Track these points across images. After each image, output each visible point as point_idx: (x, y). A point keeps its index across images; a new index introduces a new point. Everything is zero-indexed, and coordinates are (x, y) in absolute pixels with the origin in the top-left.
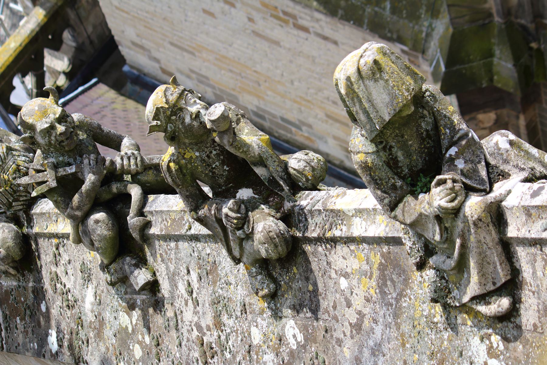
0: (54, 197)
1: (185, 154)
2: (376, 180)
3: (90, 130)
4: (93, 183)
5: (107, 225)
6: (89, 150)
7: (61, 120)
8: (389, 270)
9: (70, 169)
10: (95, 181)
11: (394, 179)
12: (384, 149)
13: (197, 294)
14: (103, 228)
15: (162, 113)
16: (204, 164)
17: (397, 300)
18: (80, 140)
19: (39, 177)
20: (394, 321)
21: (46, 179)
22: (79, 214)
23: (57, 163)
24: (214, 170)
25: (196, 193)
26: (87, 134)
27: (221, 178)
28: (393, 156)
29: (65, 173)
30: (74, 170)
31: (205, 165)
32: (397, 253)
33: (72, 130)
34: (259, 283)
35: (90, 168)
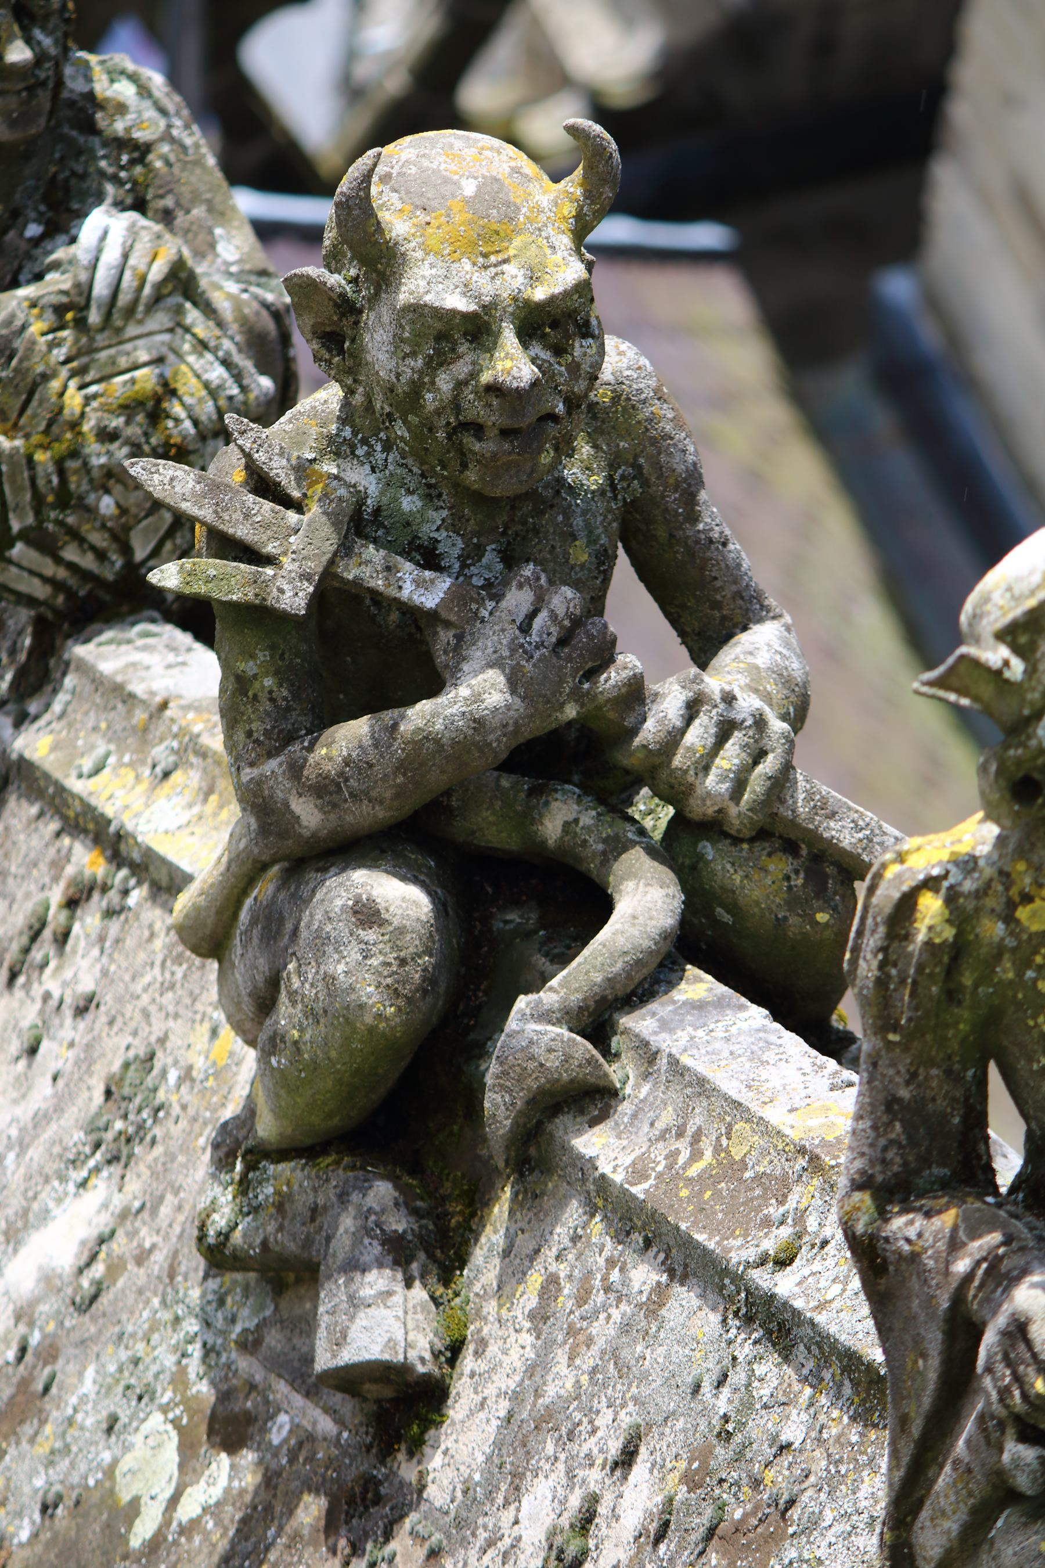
0: (253, 656)
1: (1027, 899)
4: (479, 724)
5: (403, 962)
6: (566, 556)
7: (541, 326)
10: (496, 722)
14: (375, 962)
18: (561, 481)
19: (247, 516)
21: (270, 548)
23: (377, 511)
26: (610, 478)
29: (379, 583)
30: (430, 601)
33: (560, 408)
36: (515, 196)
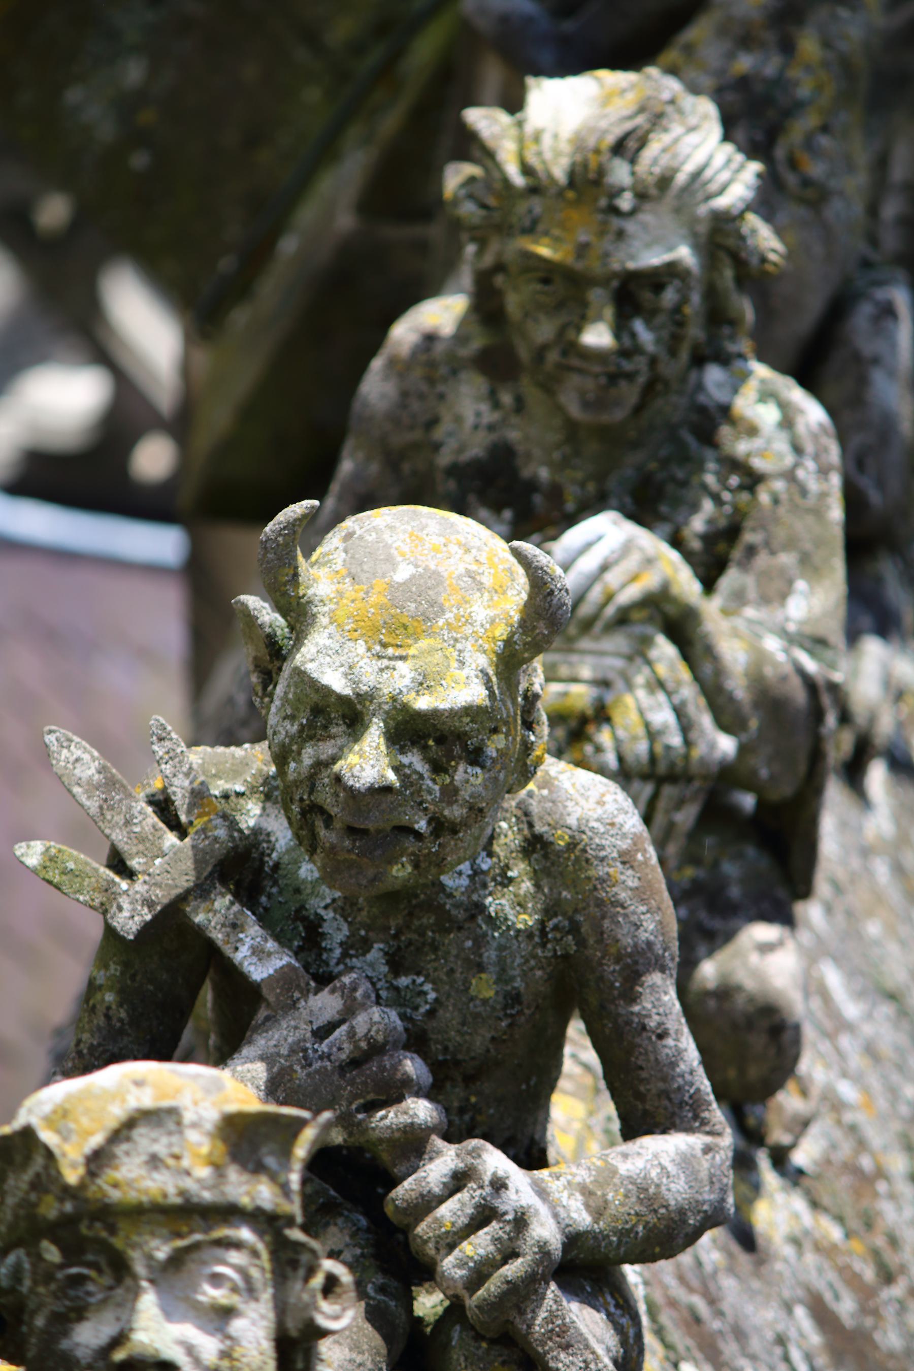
3: (574, 929)
7: (427, 736)
18: (480, 908)
19: (127, 823)
21: (135, 863)
23: (277, 866)
26: (542, 923)
29: (218, 936)
30: (258, 972)
35: (297, 1048)
36: (449, 600)
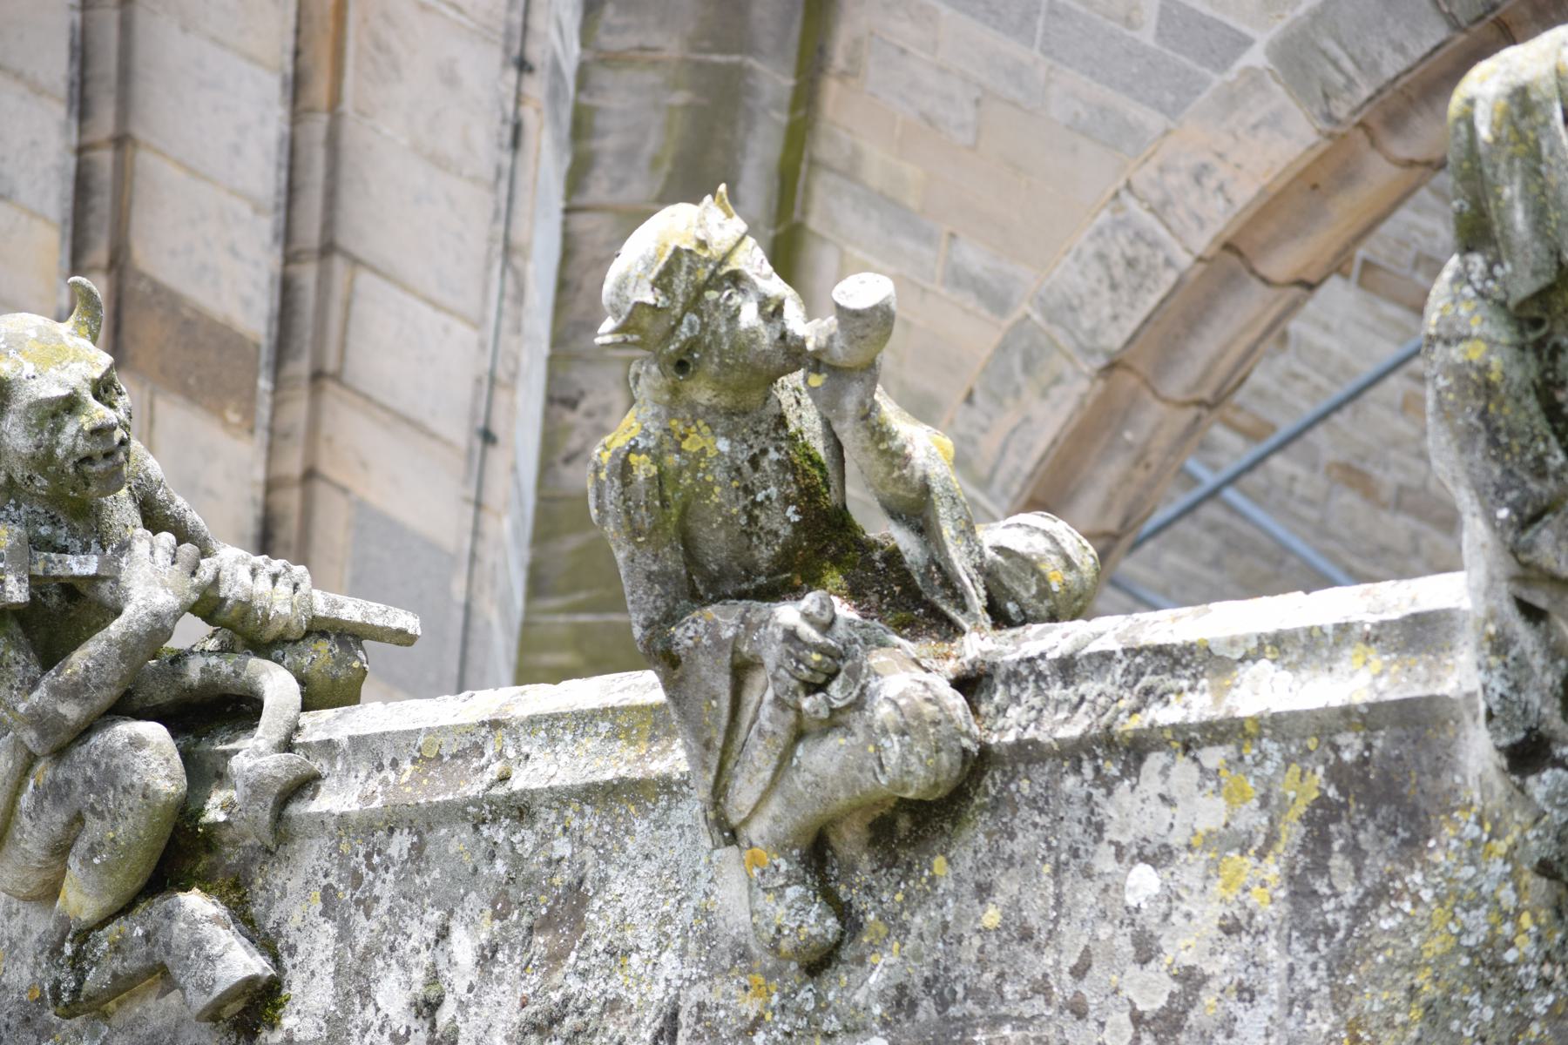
1: (684, 437)
2: (1498, 430)
8: (1350, 819)
9: (79, 562)
11: (1546, 440)
12: (1539, 345)
13: (462, 1006)
15: (684, 269)
16: (735, 484)
17: (1358, 913)
20: (1330, 985)
22: (69, 716)
24: (757, 512)
25: (677, 572)
27: (767, 545)
28: (1556, 376)
31: (738, 488)
32: (1399, 758)
34: (789, 908)
